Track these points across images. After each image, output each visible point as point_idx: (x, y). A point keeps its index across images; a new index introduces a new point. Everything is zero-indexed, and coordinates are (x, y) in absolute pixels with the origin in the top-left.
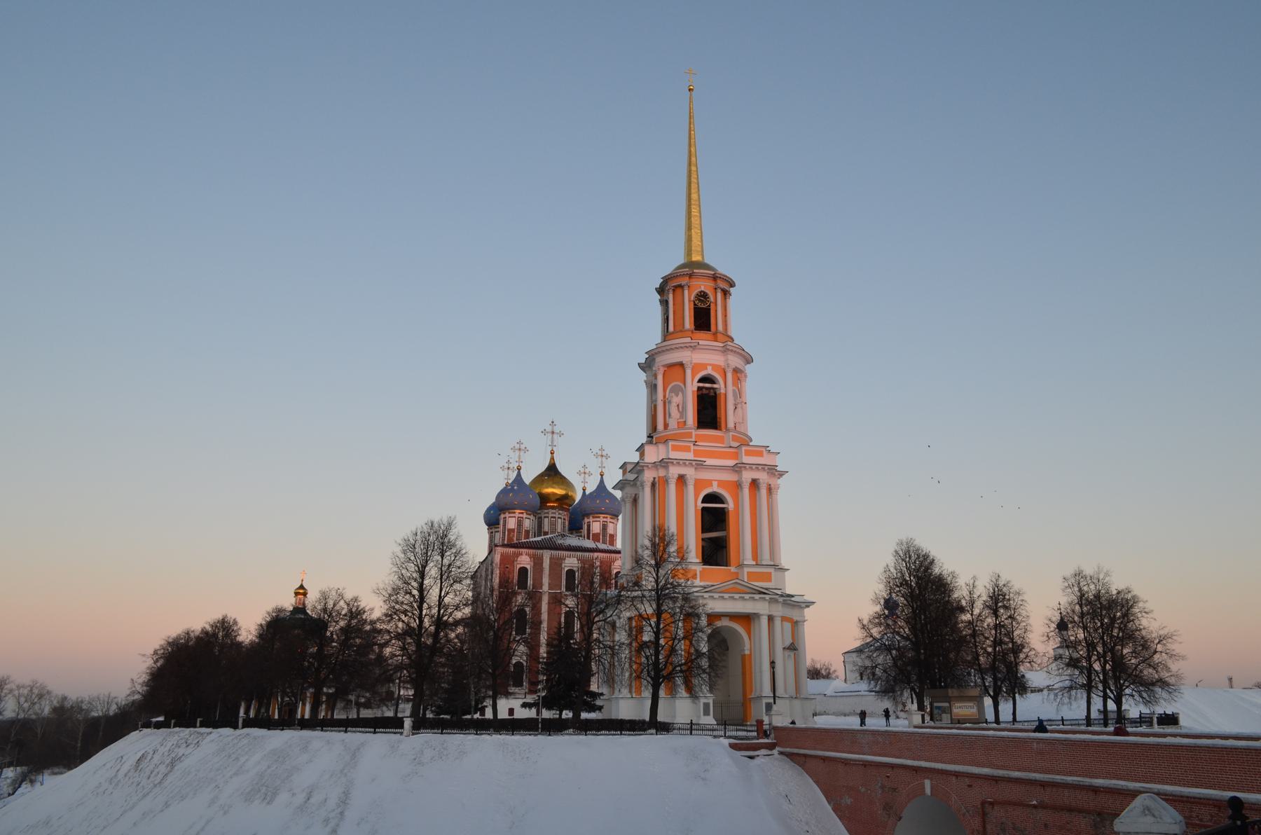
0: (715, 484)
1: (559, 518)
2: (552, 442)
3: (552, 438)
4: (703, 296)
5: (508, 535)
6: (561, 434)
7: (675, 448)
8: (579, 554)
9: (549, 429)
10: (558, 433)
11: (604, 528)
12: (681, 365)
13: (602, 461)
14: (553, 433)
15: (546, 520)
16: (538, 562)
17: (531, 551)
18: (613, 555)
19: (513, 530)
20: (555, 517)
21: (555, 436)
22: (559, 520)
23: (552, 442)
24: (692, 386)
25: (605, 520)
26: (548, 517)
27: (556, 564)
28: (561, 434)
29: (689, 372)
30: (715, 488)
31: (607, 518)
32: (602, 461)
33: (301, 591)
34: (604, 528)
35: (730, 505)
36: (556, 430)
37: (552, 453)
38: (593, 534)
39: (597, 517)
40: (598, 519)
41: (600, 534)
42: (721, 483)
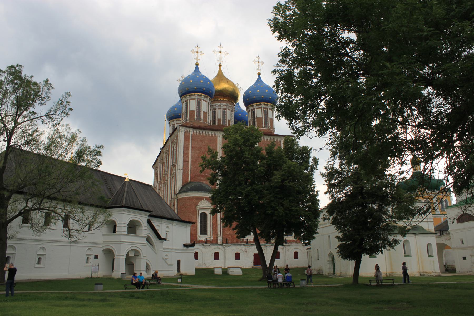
1: (228, 109)
3: (220, 55)
6: (226, 53)
9: (218, 49)
10: (224, 53)
11: (266, 113)
13: (259, 65)
14: (220, 52)
15: (219, 110)
20: (226, 109)
21: (222, 54)
22: (229, 111)
25: (266, 107)
26: (220, 109)
28: (226, 53)
31: (267, 105)
32: (259, 65)
36: (223, 50)
37: (220, 66)
38: (257, 118)
39: (259, 105)
40: (260, 106)
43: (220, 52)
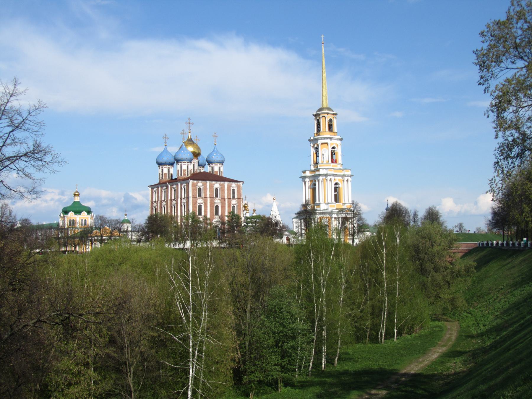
0: (337, 180)
2: (189, 127)
4: (331, 120)
5: (184, 172)
6: (193, 124)
7: (329, 171)
8: (220, 183)
9: (188, 121)
12: (327, 143)
14: (189, 123)
16: (205, 186)
17: (202, 182)
18: (231, 183)
19: (184, 170)
21: (190, 125)
23: (189, 127)
24: (330, 149)
27: (211, 186)
28: (193, 124)
29: (329, 146)
30: (337, 181)
33: (77, 193)
34: (219, 168)
35: (340, 186)
36: (191, 122)
41: (217, 171)
42: (339, 180)
43: (189, 123)
